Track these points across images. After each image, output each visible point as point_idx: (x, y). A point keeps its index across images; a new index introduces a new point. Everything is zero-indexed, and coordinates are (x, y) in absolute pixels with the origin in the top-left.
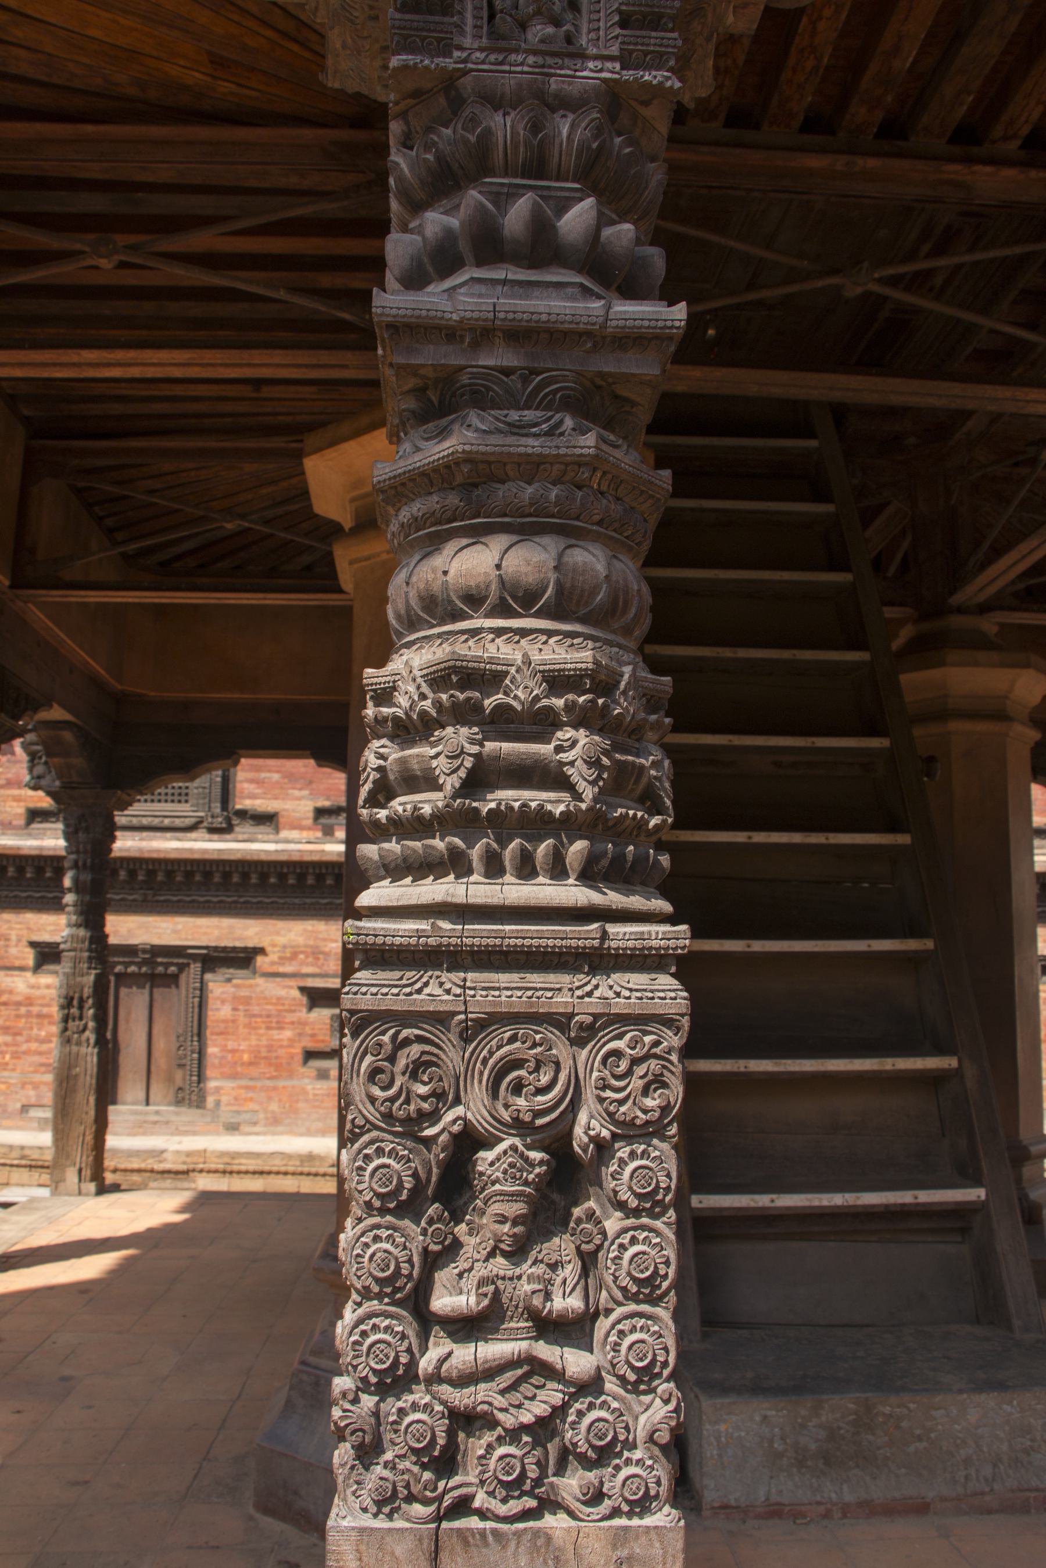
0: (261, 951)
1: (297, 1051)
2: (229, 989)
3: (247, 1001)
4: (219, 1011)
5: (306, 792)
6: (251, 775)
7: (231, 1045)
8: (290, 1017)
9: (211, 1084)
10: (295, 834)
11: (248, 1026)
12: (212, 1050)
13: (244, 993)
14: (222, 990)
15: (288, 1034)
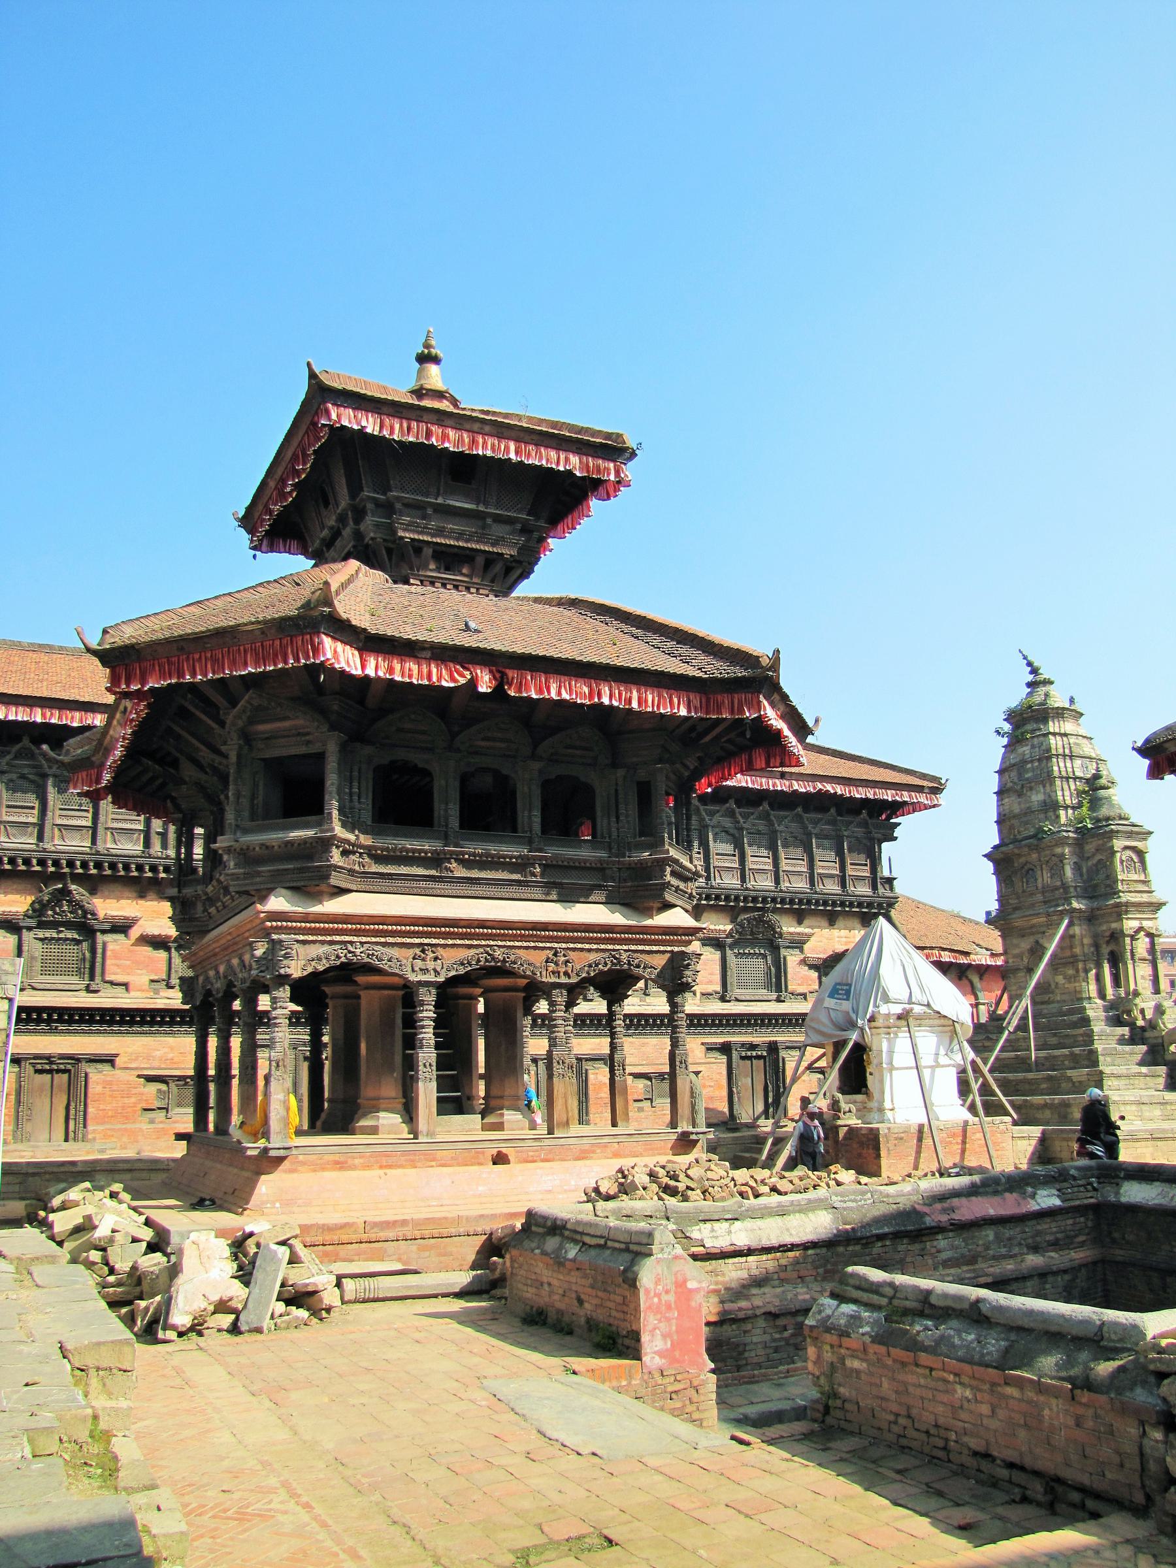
0: (117, 1055)
1: (140, 1106)
2: (100, 1076)
3: (110, 1083)
4: (95, 1088)
5: (144, 971)
6: (113, 961)
7: (102, 1107)
8: (134, 1091)
9: (90, 1128)
10: (138, 994)
11: (111, 1096)
12: (90, 1110)
13: (109, 1078)
14: (97, 1076)
15: (133, 1100)
